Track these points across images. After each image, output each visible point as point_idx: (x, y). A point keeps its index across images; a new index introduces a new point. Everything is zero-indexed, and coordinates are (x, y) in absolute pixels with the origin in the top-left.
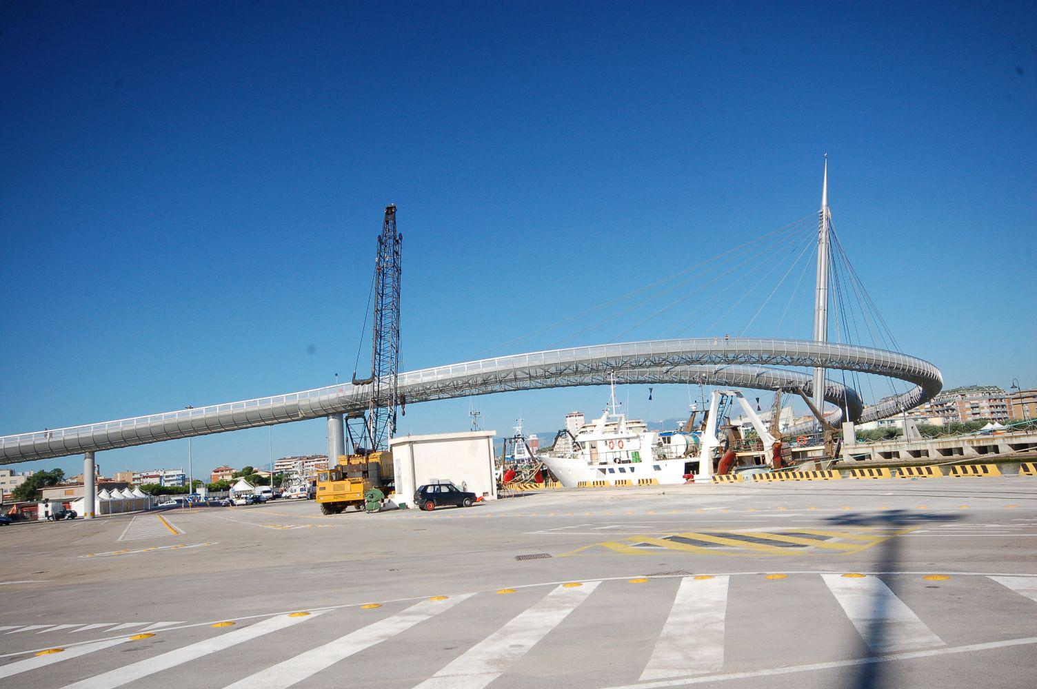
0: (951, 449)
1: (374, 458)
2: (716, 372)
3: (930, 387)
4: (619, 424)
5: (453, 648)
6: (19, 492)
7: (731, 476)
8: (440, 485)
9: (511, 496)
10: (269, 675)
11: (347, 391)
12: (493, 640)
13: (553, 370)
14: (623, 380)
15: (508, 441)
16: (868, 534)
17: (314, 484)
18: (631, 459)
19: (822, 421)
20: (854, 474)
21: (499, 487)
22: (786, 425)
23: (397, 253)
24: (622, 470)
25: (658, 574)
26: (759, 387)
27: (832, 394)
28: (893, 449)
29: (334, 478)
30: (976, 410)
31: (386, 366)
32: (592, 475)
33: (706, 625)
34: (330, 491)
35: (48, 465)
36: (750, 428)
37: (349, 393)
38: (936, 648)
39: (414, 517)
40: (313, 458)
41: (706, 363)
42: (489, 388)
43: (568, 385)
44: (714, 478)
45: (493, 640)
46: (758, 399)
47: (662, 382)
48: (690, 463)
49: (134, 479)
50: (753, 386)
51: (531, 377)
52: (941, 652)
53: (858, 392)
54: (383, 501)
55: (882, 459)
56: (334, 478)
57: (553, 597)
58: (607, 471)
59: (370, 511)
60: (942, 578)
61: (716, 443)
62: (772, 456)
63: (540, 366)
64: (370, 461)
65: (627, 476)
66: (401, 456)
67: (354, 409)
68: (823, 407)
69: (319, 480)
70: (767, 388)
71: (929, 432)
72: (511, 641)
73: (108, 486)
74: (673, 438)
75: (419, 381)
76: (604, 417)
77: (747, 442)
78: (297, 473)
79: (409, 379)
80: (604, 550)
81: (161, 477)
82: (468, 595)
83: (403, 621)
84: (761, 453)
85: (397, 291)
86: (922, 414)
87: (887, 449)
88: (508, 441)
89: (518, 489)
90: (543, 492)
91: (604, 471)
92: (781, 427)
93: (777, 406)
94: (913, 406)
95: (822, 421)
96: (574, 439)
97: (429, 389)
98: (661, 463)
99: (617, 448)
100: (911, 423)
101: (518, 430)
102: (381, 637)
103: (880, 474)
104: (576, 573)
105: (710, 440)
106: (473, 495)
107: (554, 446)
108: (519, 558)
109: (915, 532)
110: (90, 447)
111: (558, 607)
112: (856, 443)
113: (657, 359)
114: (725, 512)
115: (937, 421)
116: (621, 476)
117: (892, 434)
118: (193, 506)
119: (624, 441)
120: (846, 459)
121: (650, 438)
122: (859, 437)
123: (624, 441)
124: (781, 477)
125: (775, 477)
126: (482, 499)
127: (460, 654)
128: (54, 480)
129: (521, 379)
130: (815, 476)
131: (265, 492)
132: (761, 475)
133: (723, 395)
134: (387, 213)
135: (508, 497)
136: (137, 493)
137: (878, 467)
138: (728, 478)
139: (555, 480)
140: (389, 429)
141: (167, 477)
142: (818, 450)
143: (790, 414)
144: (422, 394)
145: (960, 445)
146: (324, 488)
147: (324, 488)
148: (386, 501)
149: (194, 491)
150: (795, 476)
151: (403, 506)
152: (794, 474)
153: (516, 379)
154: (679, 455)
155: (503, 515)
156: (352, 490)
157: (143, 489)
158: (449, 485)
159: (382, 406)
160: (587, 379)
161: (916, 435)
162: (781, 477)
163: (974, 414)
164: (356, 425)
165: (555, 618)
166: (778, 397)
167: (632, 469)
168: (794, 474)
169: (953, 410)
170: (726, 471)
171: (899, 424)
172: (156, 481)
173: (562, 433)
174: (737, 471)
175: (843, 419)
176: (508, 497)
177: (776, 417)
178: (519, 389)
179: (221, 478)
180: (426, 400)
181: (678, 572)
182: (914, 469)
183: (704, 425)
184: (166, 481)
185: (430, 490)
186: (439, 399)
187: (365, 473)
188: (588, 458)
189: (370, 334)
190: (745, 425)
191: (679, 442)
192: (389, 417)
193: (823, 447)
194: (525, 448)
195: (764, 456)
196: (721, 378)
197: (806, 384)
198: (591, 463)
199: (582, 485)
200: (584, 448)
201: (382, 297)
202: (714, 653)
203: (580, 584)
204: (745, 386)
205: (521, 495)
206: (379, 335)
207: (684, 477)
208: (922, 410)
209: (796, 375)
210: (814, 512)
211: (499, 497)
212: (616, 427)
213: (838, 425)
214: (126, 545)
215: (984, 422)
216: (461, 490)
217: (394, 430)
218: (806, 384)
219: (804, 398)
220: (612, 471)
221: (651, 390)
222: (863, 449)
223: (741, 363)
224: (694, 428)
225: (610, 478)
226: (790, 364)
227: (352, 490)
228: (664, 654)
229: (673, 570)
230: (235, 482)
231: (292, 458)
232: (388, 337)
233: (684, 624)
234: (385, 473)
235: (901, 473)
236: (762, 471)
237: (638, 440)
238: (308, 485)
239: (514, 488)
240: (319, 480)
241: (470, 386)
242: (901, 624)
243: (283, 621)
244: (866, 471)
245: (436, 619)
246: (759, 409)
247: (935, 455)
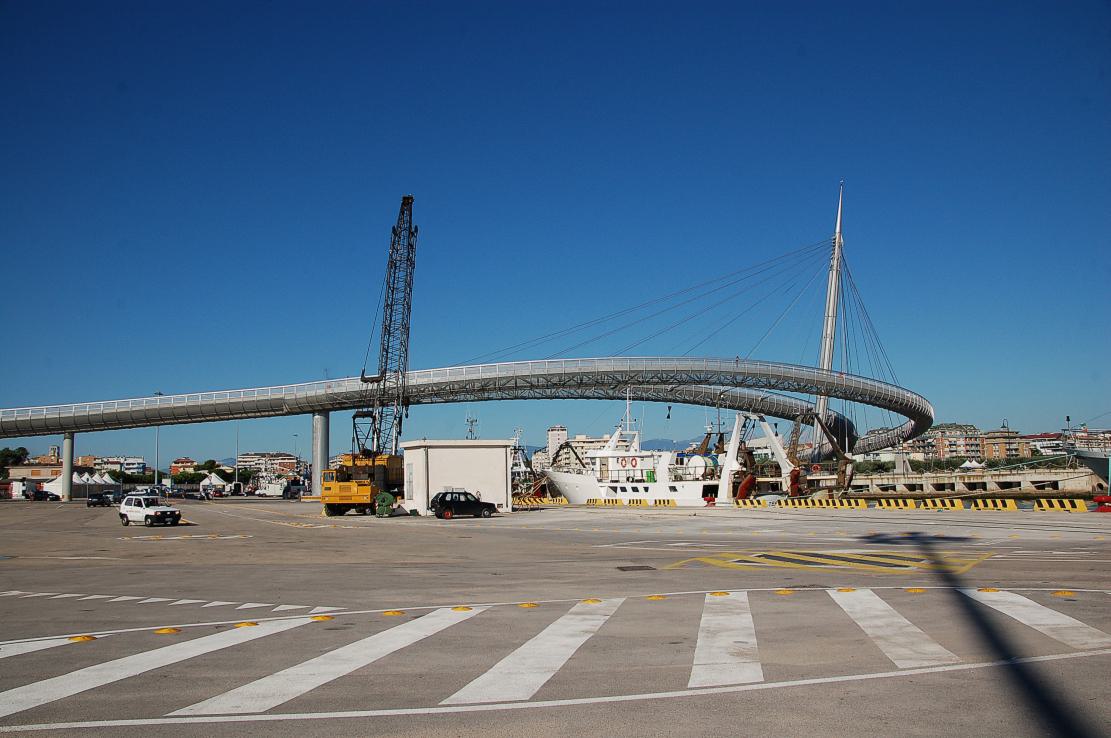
1: (381, 461)
11: (352, 385)
24: (635, 489)
32: (602, 493)
34: (337, 492)
58: (619, 490)
65: (641, 495)
67: (360, 405)
91: (615, 489)
98: (677, 484)
99: (629, 467)
105: (730, 464)
116: (636, 496)
121: (667, 458)
133: (747, 418)
136: (108, 479)
146: (330, 489)
156: (360, 492)
167: (646, 489)
172: (117, 468)
187: (371, 476)
199: (591, 503)
220: (624, 489)
227: (360, 492)
234: (392, 477)
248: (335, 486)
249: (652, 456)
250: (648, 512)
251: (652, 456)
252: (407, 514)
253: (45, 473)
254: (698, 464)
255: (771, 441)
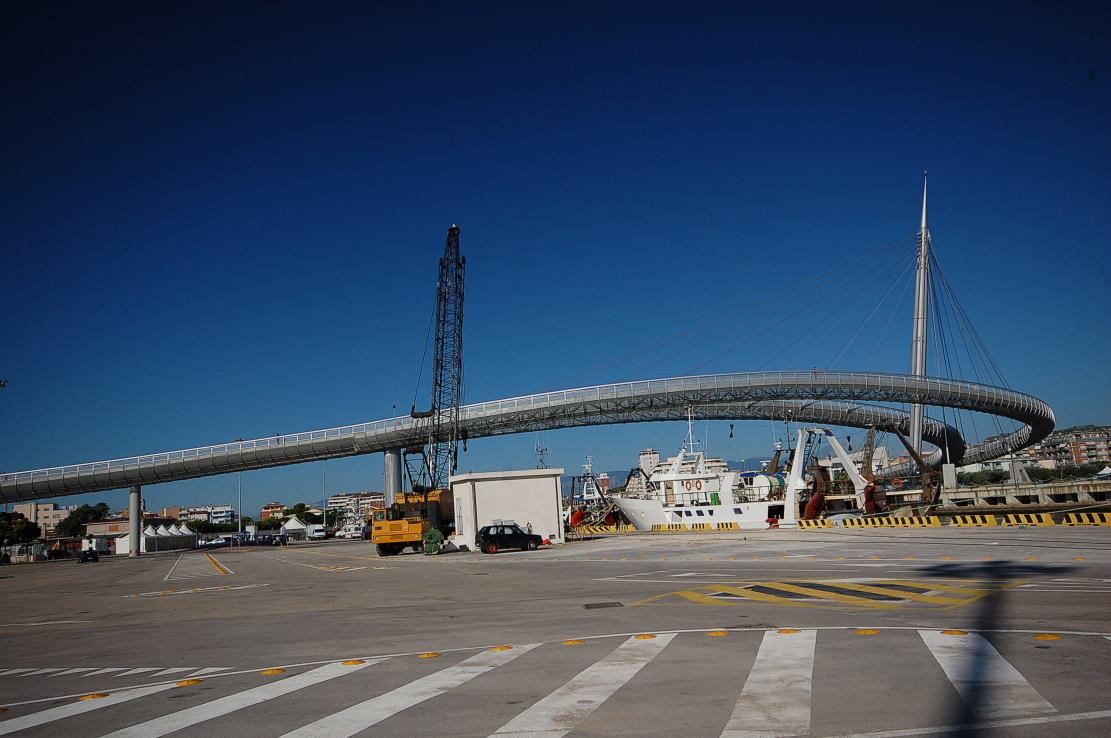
0: (1064, 495)
1: (433, 497)
2: (803, 408)
3: (1041, 426)
4: (697, 463)
5: (517, 703)
6: (62, 527)
7: (818, 521)
8: (504, 527)
9: (579, 540)
10: (322, 727)
11: (408, 424)
12: (560, 694)
13: (626, 403)
14: (701, 416)
15: (576, 480)
16: (971, 587)
17: (370, 523)
18: (709, 501)
19: (920, 462)
20: (956, 522)
21: (567, 529)
22: (880, 467)
23: (460, 278)
24: (700, 513)
25: (739, 627)
26: (850, 424)
27: (931, 433)
28: (999, 494)
29: (391, 516)
30: (1093, 453)
31: (446, 399)
32: (668, 518)
33: (791, 683)
34: (385, 531)
35: (92, 499)
36: (840, 469)
37: (407, 426)
38: (1046, 715)
39: (476, 561)
40: (368, 495)
41: (791, 398)
42: (557, 423)
43: (642, 421)
44: (800, 523)
45: (560, 694)
46: (849, 438)
47: (743, 418)
48: (775, 506)
49: (181, 516)
50: (843, 423)
51: (602, 412)
52: (1053, 719)
53: (960, 431)
54: (442, 543)
55: (987, 505)
56: (391, 516)
57: (625, 649)
58: (684, 514)
59: (429, 553)
60: (1055, 638)
61: (802, 485)
62: (864, 500)
63: (612, 400)
64: (429, 499)
65: (706, 519)
66: (462, 495)
67: (411, 444)
68: (920, 446)
69: (375, 520)
70: (859, 425)
71: (1038, 475)
72: (580, 696)
73: (155, 522)
74: (756, 480)
75: (482, 414)
76: (681, 455)
77: (837, 484)
78: (351, 511)
79: (471, 412)
80: (683, 599)
81: (209, 514)
82: (534, 646)
83: (463, 672)
84: (852, 497)
85: (460, 317)
86: (1032, 455)
87: (993, 494)
88: (576, 480)
89: (587, 532)
90: (616, 535)
91: (680, 513)
92: (874, 468)
93: (870, 447)
94: (1021, 447)
95: (920, 462)
96: (648, 478)
97: (492, 423)
98: (740, 506)
99: (694, 489)
100: (1020, 466)
101: (588, 467)
102: (441, 689)
103: (984, 521)
104: (649, 624)
105: (796, 482)
106: (540, 537)
107: (626, 486)
108: (588, 607)
109: (1024, 585)
110: (136, 481)
111: (629, 659)
112: (958, 487)
113: (738, 393)
114: (812, 560)
115: (1049, 464)
117: (998, 478)
118: (242, 545)
119: (703, 482)
120: (946, 501)
121: (730, 479)
122: (963, 480)
123: (703, 482)
124: (874, 523)
125: (867, 523)
126: (549, 543)
127: (524, 709)
128: (99, 514)
129: (591, 414)
130: (912, 522)
131: (317, 531)
132: (851, 521)
133: (811, 433)
134: (450, 235)
135: (576, 540)
136: (184, 530)
137: (982, 513)
138: (816, 524)
139: (627, 522)
140: (450, 465)
141: (215, 513)
142: (915, 494)
143: (885, 454)
144: (485, 429)
145: (1075, 490)
146: (380, 528)
147: (380, 528)
148: (446, 542)
149: (243, 529)
150: (889, 522)
151: (464, 549)
152: (888, 520)
153: (586, 413)
154: (762, 497)
155: (571, 560)
157: (190, 525)
158: (514, 527)
159: (442, 441)
160: (663, 414)
161: (1024, 479)
162: (874, 523)
163: (1091, 457)
164: (415, 460)
165: (625, 672)
166: (871, 436)
167: (711, 512)
168: (888, 520)
169: (1066, 452)
170: (814, 517)
171: (1005, 466)
172: (204, 517)
173: (635, 472)
174: (825, 516)
175: (943, 460)
176: (576, 540)
177: (869, 458)
178: (588, 424)
179: (271, 515)
180: (489, 435)
181: (761, 625)
182: (1022, 516)
183: (790, 466)
184: (214, 518)
185: (492, 532)
186: (504, 434)
187: (424, 513)
188: (664, 501)
189: (431, 363)
190: (835, 465)
191: (762, 483)
192: (450, 453)
193: (921, 491)
194: (595, 488)
195: (855, 500)
196: (809, 414)
197: (902, 422)
198: (666, 505)
199: (656, 530)
200: (659, 488)
201: (443, 325)
202: (800, 715)
203: (653, 636)
204: (835, 423)
205: (590, 539)
206: (439, 364)
207: (767, 521)
208: (1032, 452)
209: (892, 411)
210: (911, 562)
211: (567, 540)
212: (694, 466)
213: (938, 467)
214: (173, 585)
215: (1102, 466)
216: (526, 532)
217: (455, 467)
218: (902, 422)
219: (901, 438)
220: (688, 514)
221: (732, 426)
222: (965, 494)
223: (831, 398)
224: (778, 468)
225: (687, 522)
226: (884, 400)
227: (409, 530)
228: (744, 713)
229: (754, 623)
230: (287, 520)
231: (347, 495)
232: (449, 367)
233: (767, 682)
235: (1008, 521)
236: (852, 516)
237: (717, 480)
238: (363, 525)
239: (584, 531)
240: (375, 520)
241: (536, 421)
242: (1007, 687)
243: (336, 669)
244: (968, 518)
245: (497, 671)
246: (850, 449)
247: (1045, 501)
248: (386, 525)
249: (718, 477)
250: (712, 536)
251: (718, 477)
252: (457, 551)
253: (121, 525)
254: (762, 483)
255: (843, 457)
